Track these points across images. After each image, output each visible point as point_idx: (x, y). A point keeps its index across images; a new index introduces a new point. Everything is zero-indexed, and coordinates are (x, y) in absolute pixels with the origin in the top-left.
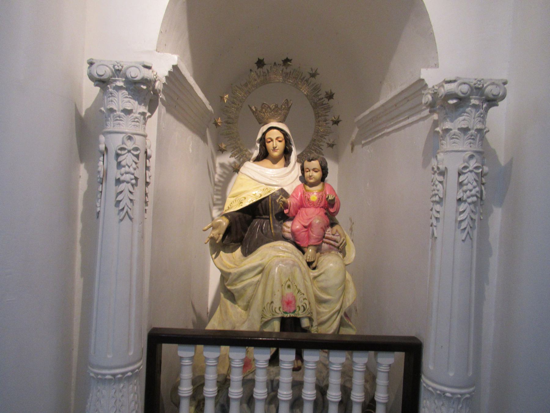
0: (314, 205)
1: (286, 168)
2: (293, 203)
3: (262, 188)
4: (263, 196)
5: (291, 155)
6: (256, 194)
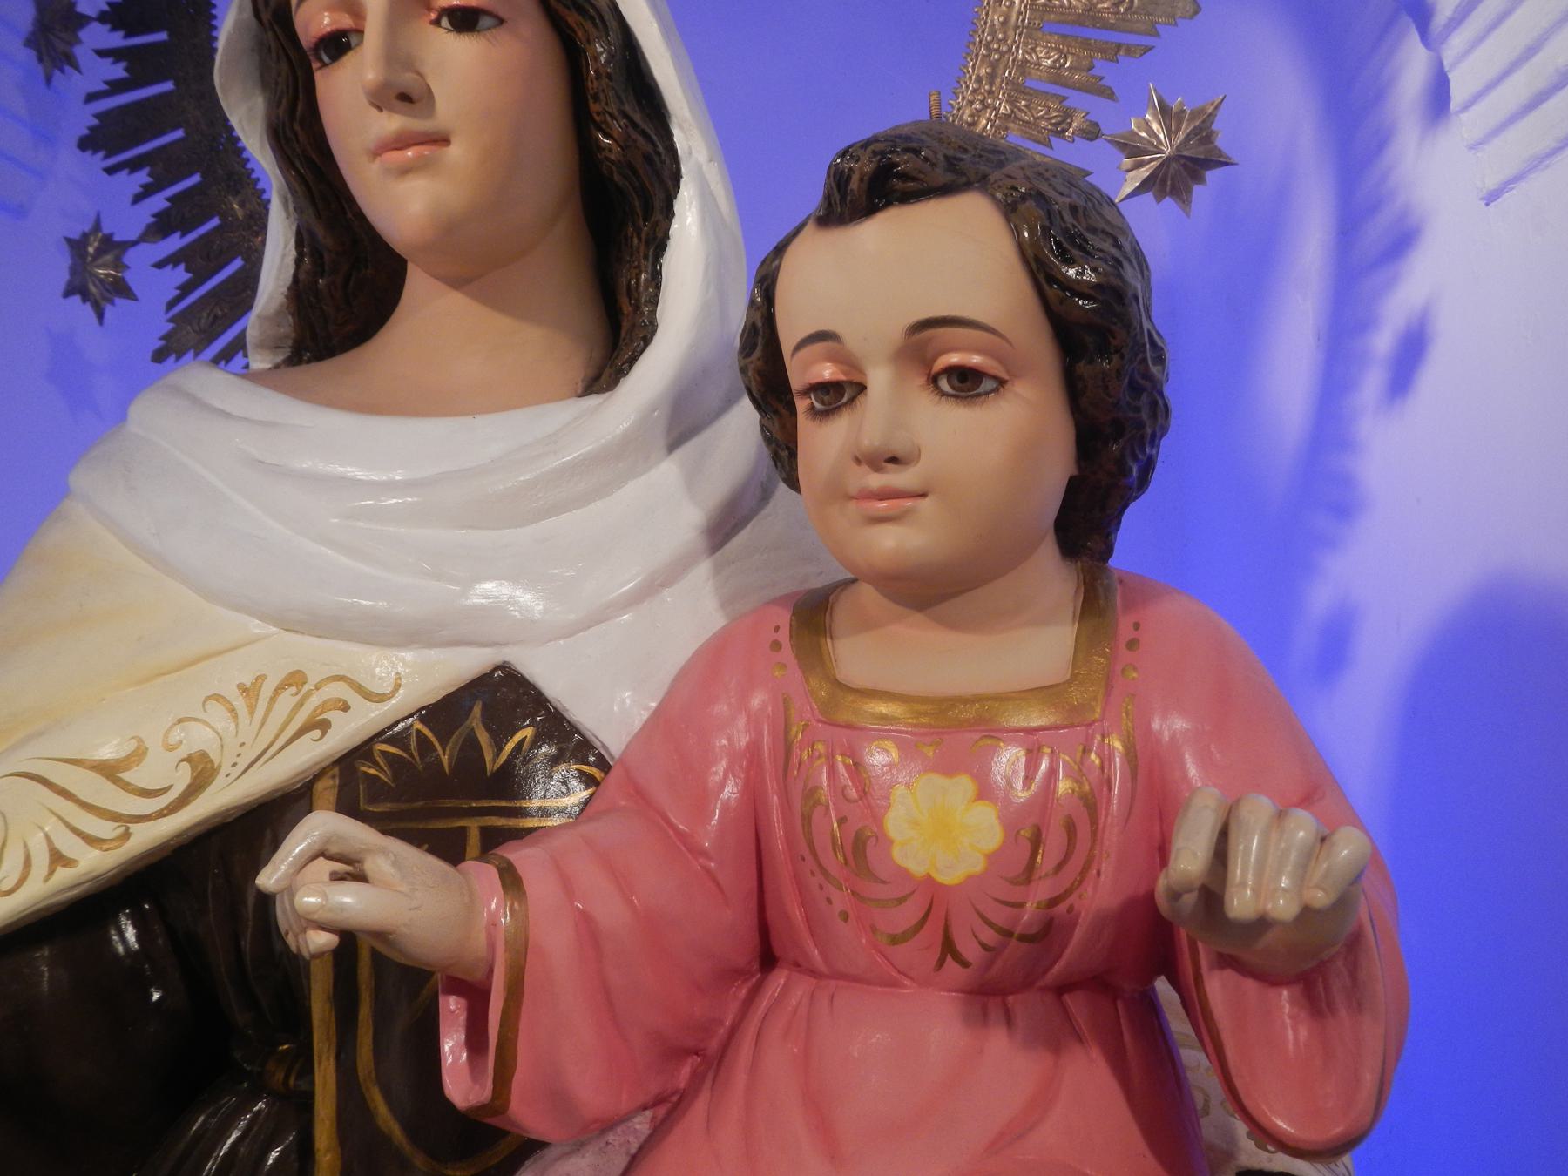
0: (949, 948)
1: (593, 400)
2: (588, 930)
3: (230, 676)
4: (220, 780)
5: (659, 244)
6: (137, 756)
